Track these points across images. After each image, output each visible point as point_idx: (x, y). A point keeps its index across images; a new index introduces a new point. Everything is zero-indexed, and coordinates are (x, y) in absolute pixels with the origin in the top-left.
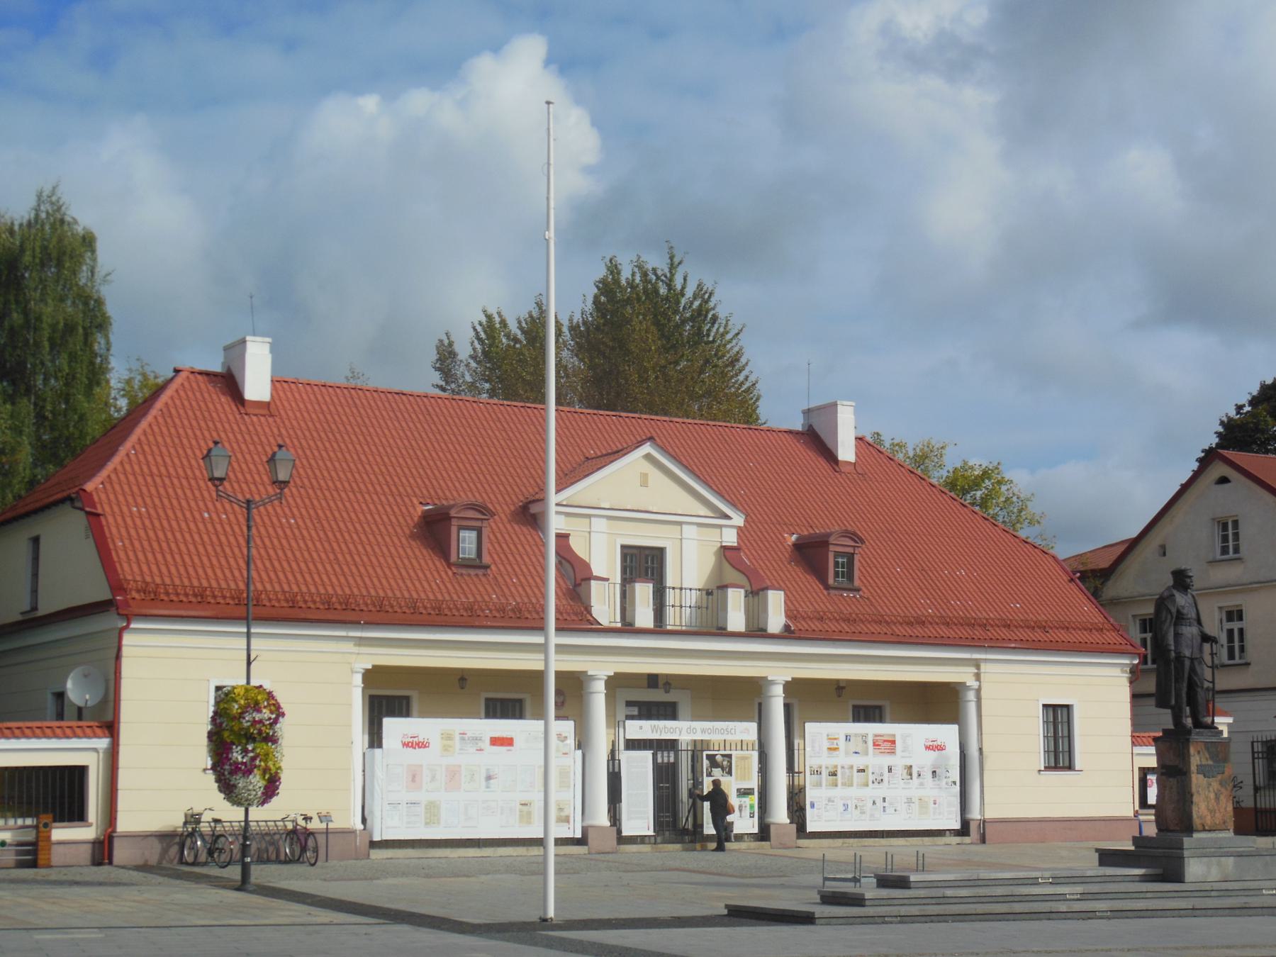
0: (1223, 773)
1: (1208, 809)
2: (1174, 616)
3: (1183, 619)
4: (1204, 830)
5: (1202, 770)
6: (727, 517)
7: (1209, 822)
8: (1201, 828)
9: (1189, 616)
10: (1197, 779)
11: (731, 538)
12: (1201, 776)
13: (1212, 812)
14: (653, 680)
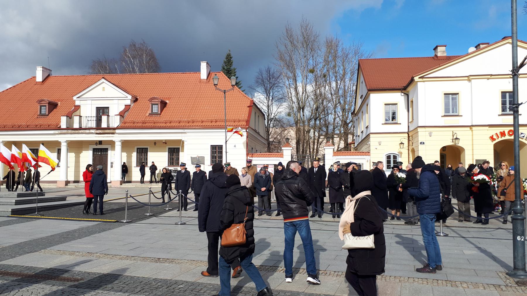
6: (127, 97)
11: (128, 102)
14: (100, 142)
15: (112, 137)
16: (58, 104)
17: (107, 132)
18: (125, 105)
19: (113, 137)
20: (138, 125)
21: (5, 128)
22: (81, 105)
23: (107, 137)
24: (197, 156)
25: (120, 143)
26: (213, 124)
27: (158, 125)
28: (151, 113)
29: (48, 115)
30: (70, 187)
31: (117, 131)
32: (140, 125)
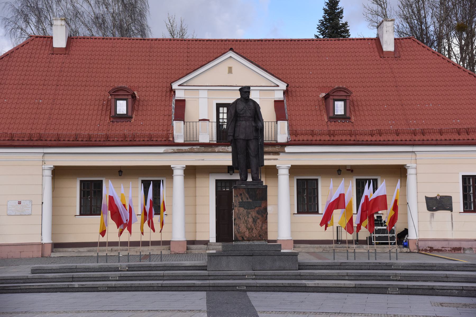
0: (260, 206)
1: (247, 228)
2: (233, 115)
3: (240, 117)
4: (243, 240)
5: (242, 205)
6: (278, 86)
7: (247, 236)
8: (240, 239)
9: (244, 115)
10: (239, 210)
11: (279, 96)
12: (242, 209)
13: (250, 229)
15: (274, 159)
16: (135, 96)
17: (268, 151)
18: (276, 102)
19: (277, 159)
21: (60, 142)
22: (186, 99)
24: (438, 195)
26: (463, 137)
28: (331, 115)
29: (131, 118)
30: (197, 252)
31: (288, 149)
32: (327, 138)
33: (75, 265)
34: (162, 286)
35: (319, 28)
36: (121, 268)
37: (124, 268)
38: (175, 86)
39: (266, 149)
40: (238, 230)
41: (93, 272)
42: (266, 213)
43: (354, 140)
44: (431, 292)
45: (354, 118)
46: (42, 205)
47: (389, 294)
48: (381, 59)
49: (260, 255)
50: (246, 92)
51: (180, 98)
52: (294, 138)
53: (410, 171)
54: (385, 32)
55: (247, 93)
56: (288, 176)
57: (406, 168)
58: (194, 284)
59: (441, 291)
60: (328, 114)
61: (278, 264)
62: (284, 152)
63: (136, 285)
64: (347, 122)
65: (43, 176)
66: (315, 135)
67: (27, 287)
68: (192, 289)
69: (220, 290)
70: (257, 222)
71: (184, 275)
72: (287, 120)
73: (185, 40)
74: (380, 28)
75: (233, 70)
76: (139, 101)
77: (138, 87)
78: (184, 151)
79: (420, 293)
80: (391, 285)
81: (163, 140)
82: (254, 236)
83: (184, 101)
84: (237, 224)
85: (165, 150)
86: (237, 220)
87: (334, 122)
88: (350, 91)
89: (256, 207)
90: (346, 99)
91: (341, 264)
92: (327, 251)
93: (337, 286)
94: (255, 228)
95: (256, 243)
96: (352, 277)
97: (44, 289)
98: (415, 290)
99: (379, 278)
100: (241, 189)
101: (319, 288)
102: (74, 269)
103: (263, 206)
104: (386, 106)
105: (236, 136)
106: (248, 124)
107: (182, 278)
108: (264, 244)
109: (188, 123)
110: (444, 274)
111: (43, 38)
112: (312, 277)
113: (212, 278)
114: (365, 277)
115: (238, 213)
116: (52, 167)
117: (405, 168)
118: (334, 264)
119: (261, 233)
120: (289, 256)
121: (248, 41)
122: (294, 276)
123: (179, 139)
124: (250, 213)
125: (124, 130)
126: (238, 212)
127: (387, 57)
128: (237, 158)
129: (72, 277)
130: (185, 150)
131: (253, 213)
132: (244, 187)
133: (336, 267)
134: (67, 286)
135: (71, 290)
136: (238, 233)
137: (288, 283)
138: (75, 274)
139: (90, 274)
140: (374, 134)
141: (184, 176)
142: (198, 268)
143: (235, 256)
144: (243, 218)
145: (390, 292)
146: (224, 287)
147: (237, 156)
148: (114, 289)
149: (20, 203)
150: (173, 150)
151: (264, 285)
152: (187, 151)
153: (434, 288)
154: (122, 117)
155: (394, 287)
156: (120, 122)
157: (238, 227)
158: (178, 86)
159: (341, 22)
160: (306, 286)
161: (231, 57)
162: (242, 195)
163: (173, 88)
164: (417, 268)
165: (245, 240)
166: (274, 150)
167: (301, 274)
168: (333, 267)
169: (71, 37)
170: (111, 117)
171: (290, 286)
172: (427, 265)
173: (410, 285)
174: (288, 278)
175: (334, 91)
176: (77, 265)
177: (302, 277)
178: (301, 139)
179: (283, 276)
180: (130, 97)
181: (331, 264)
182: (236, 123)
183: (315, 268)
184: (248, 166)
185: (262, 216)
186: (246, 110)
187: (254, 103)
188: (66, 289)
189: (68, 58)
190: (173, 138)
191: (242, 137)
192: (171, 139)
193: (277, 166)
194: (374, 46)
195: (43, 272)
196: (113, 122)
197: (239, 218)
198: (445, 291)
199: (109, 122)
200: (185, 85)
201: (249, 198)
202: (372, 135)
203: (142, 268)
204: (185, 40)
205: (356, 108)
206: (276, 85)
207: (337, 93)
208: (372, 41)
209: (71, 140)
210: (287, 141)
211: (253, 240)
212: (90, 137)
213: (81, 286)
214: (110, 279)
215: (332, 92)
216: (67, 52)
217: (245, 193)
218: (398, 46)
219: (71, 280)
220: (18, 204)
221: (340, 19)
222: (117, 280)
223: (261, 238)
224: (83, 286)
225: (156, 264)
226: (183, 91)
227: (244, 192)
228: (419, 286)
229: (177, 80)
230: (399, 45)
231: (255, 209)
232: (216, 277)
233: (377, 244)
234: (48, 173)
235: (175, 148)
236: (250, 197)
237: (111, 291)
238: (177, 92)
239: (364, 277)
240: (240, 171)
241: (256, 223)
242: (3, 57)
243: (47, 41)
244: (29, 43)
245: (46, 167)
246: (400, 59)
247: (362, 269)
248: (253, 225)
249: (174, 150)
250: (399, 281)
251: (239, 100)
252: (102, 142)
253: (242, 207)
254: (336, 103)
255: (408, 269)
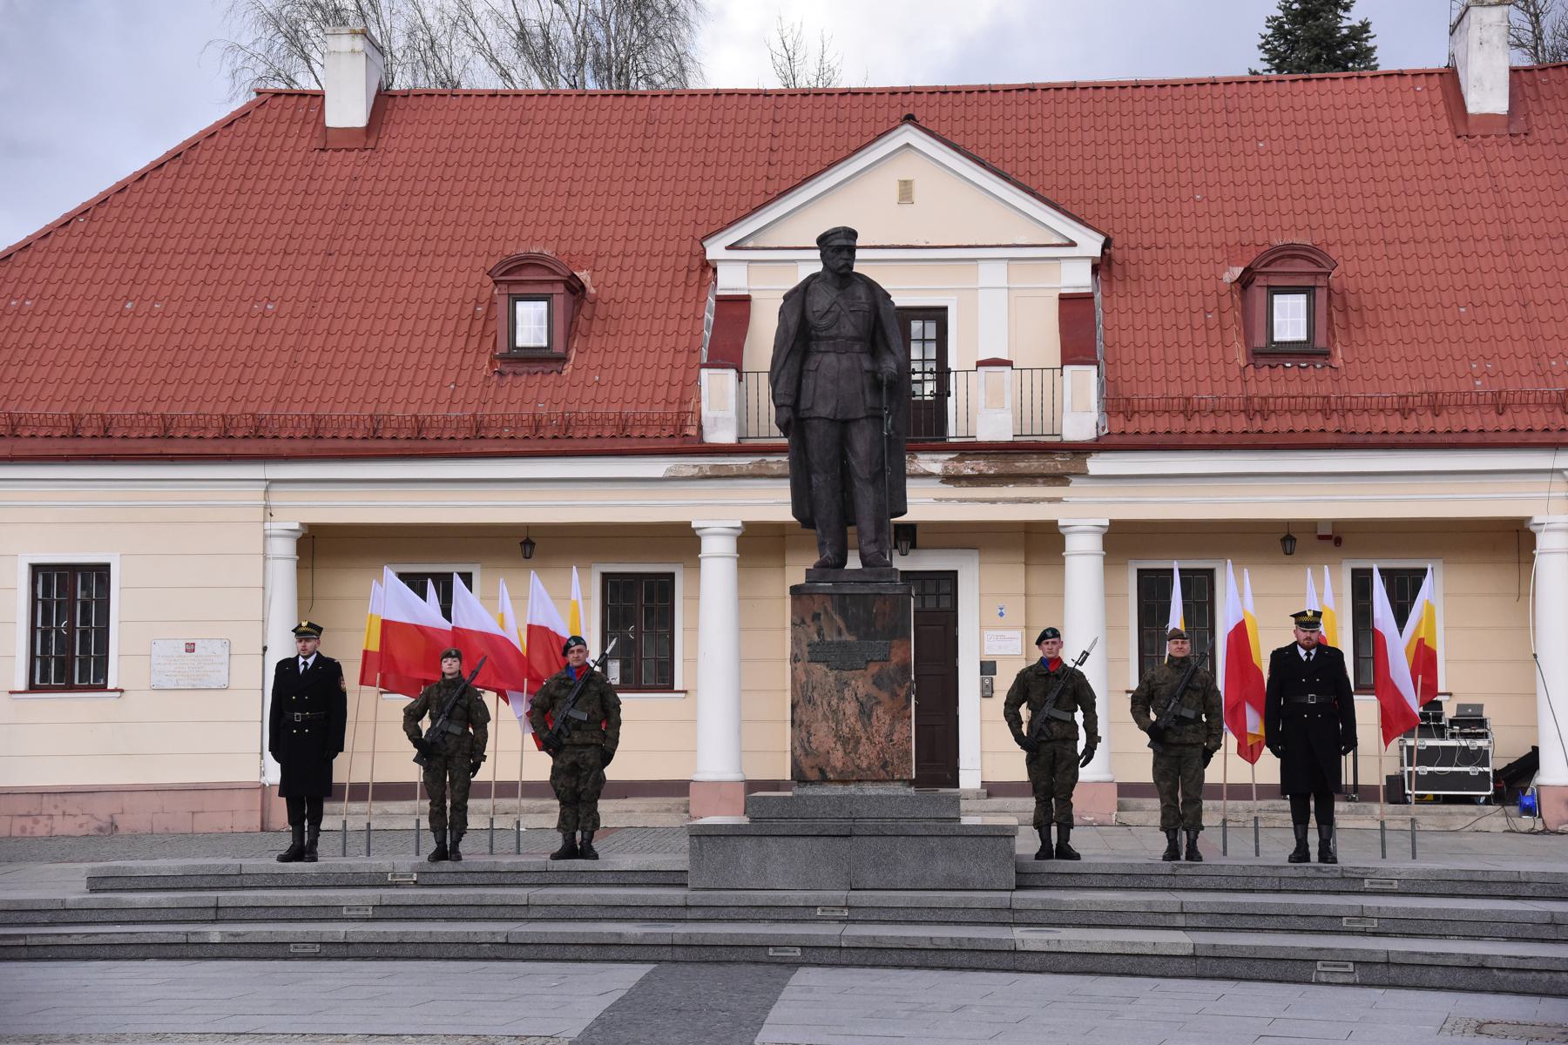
0: (886, 660)
1: (838, 737)
3: (819, 338)
4: (824, 780)
6: (1072, 244)
7: (839, 765)
8: (813, 775)
9: (833, 332)
10: (807, 672)
11: (1079, 278)
12: (818, 666)
13: (850, 742)
16: (583, 287)
18: (1064, 299)
19: (1059, 500)
20: (1224, 424)
21: (319, 444)
22: (754, 296)
23: (1019, 501)
25: (1094, 543)
27: (1363, 423)
28: (1260, 342)
29: (563, 359)
31: (1098, 464)
32: (1241, 423)
33: (237, 862)
34: (507, 943)
35: (1267, 47)
36: (393, 876)
37: (401, 876)
38: (715, 249)
39: (1022, 464)
40: (807, 745)
41: (300, 887)
42: (908, 684)
43: (1339, 431)
44: (1475, 978)
45: (1342, 349)
46: (263, 655)
47: (1319, 983)
48: (1458, 142)
49: (876, 833)
50: (840, 249)
51: (733, 289)
52: (1120, 424)
53: (1543, 541)
54: (1474, 45)
55: (845, 255)
56: (1100, 559)
57: (1533, 528)
58: (620, 935)
59: (1512, 976)
60: (1248, 337)
61: (941, 867)
62: (1084, 474)
63: (418, 939)
64: (1318, 366)
65: (265, 558)
66: (1197, 414)
67: (50, 940)
68: (613, 953)
69: (711, 958)
70: (874, 717)
71: (598, 901)
72: (1097, 363)
73: (766, 95)
74: (1460, 33)
75: (918, 192)
76: (594, 303)
77: (593, 256)
78: (735, 472)
79: (1435, 983)
80: (1328, 949)
81: (666, 434)
82: (864, 765)
83: (745, 300)
84: (802, 722)
85: (669, 470)
86: (803, 710)
87: (1270, 366)
88: (1327, 257)
89: (871, 661)
90: (1312, 284)
91: (1175, 870)
92: (1236, 824)
93: (1128, 950)
94: (868, 738)
95: (871, 790)
96: (1201, 918)
97: (107, 948)
98: (1417, 970)
99: (1301, 924)
100: (816, 597)
101: (1064, 958)
102: (232, 878)
103: (895, 660)
104: (1463, 310)
105: (802, 407)
106: (846, 362)
107: (593, 916)
108: (897, 796)
109: (752, 377)
110: (1543, 914)
111: (296, 97)
112: (1054, 918)
113: (699, 914)
114: (1251, 918)
115: (807, 682)
116: (296, 526)
117: (1528, 530)
118: (1149, 871)
119: (887, 756)
120: (984, 839)
121: (984, 91)
122: (989, 912)
123: (721, 432)
124: (850, 685)
125: (537, 402)
126: (804, 679)
127: (1483, 136)
128: (810, 487)
129: (213, 905)
130: (739, 467)
131: (861, 684)
132: (827, 591)
133: (1158, 882)
134: (183, 939)
135: (197, 951)
136: (807, 755)
137: (952, 939)
138: (226, 897)
139: (277, 897)
140: (1414, 410)
141: (738, 559)
142: (661, 878)
143: (787, 838)
144: (825, 702)
145: (1323, 975)
146: (724, 950)
147: (809, 479)
148: (343, 950)
149: (190, 648)
150: (696, 470)
151: (867, 945)
152: (744, 471)
153: (1489, 965)
154: (531, 357)
155: (1337, 959)
156: (525, 375)
157: (804, 734)
158: (727, 248)
159: (1345, 23)
160: (1015, 951)
161: (908, 145)
162: (822, 617)
163: (709, 257)
164: (1460, 889)
165: (830, 781)
166: (1050, 467)
167: (1014, 906)
168: (1145, 883)
169: (390, 93)
170: (496, 357)
171: (956, 950)
172: (1495, 879)
173: (1398, 952)
174: (968, 918)
175: (1271, 258)
176: (245, 862)
177: (1016, 915)
178: (1146, 428)
179: (949, 912)
180: (560, 288)
181: (1137, 871)
182: (803, 361)
183: (1079, 884)
184: (847, 516)
185: (894, 695)
186: (839, 314)
187: (872, 286)
188: (181, 947)
189: (372, 162)
190: (700, 428)
191: (825, 409)
192: (692, 431)
193: (1060, 524)
194: (1438, 95)
195: (129, 885)
196: (501, 373)
197: (809, 702)
198: (1530, 976)
199: (490, 374)
200: (750, 244)
201: (844, 630)
202: (1405, 412)
203: (466, 876)
204: (766, 95)
205: (1353, 317)
206: (1066, 242)
207: (1280, 265)
208: (1431, 79)
209: (358, 436)
210: (1094, 436)
211: (860, 781)
212: (420, 428)
213: (231, 940)
214: (344, 913)
215: (1264, 263)
216: (371, 144)
217: (833, 613)
218: (1524, 94)
219: (211, 914)
220: (187, 651)
221: (1340, 12)
222: (368, 920)
223: (887, 772)
224: (237, 940)
225: (516, 863)
226: (744, 267)
227: (829, 609)
228: (1431, 954)
229: (722, 230)
230: (1529, 91)
231: (866, 669)
232: (712, 913)
233: (1421, 800)
234: (285, 549)
235: (706, 462)
236: (847, 627)
237: (329, 958)
238: (722, 271)
239: (1244, 917)
240: (819, 531)
241: (869, 720)
242: (163, 164)
243: (308, 109)
244: (250, 115)
245: (276, 526)
246: (1530, 139)
247: (1252, 891)
248: (859, 726)
249: (701, 468)
250: (1375, 934)
251: (817, 280)
252: (457, 443)
253: (818, 662)
254: (1278, 299)
255: (1424, 891)
